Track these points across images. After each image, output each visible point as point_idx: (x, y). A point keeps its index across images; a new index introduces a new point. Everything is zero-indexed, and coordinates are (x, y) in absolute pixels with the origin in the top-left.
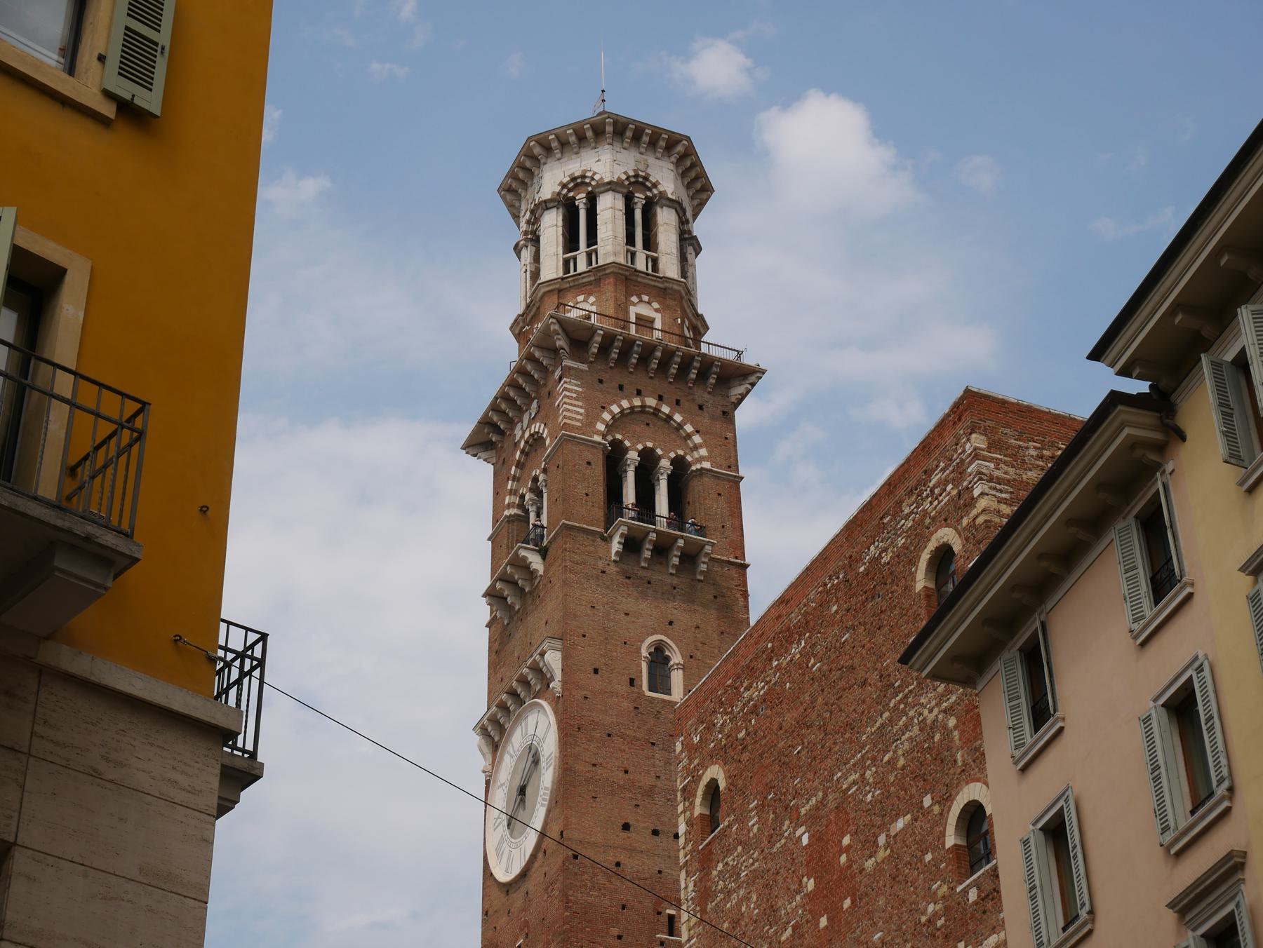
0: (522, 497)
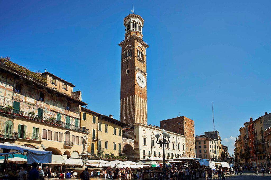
0: (126, 52)
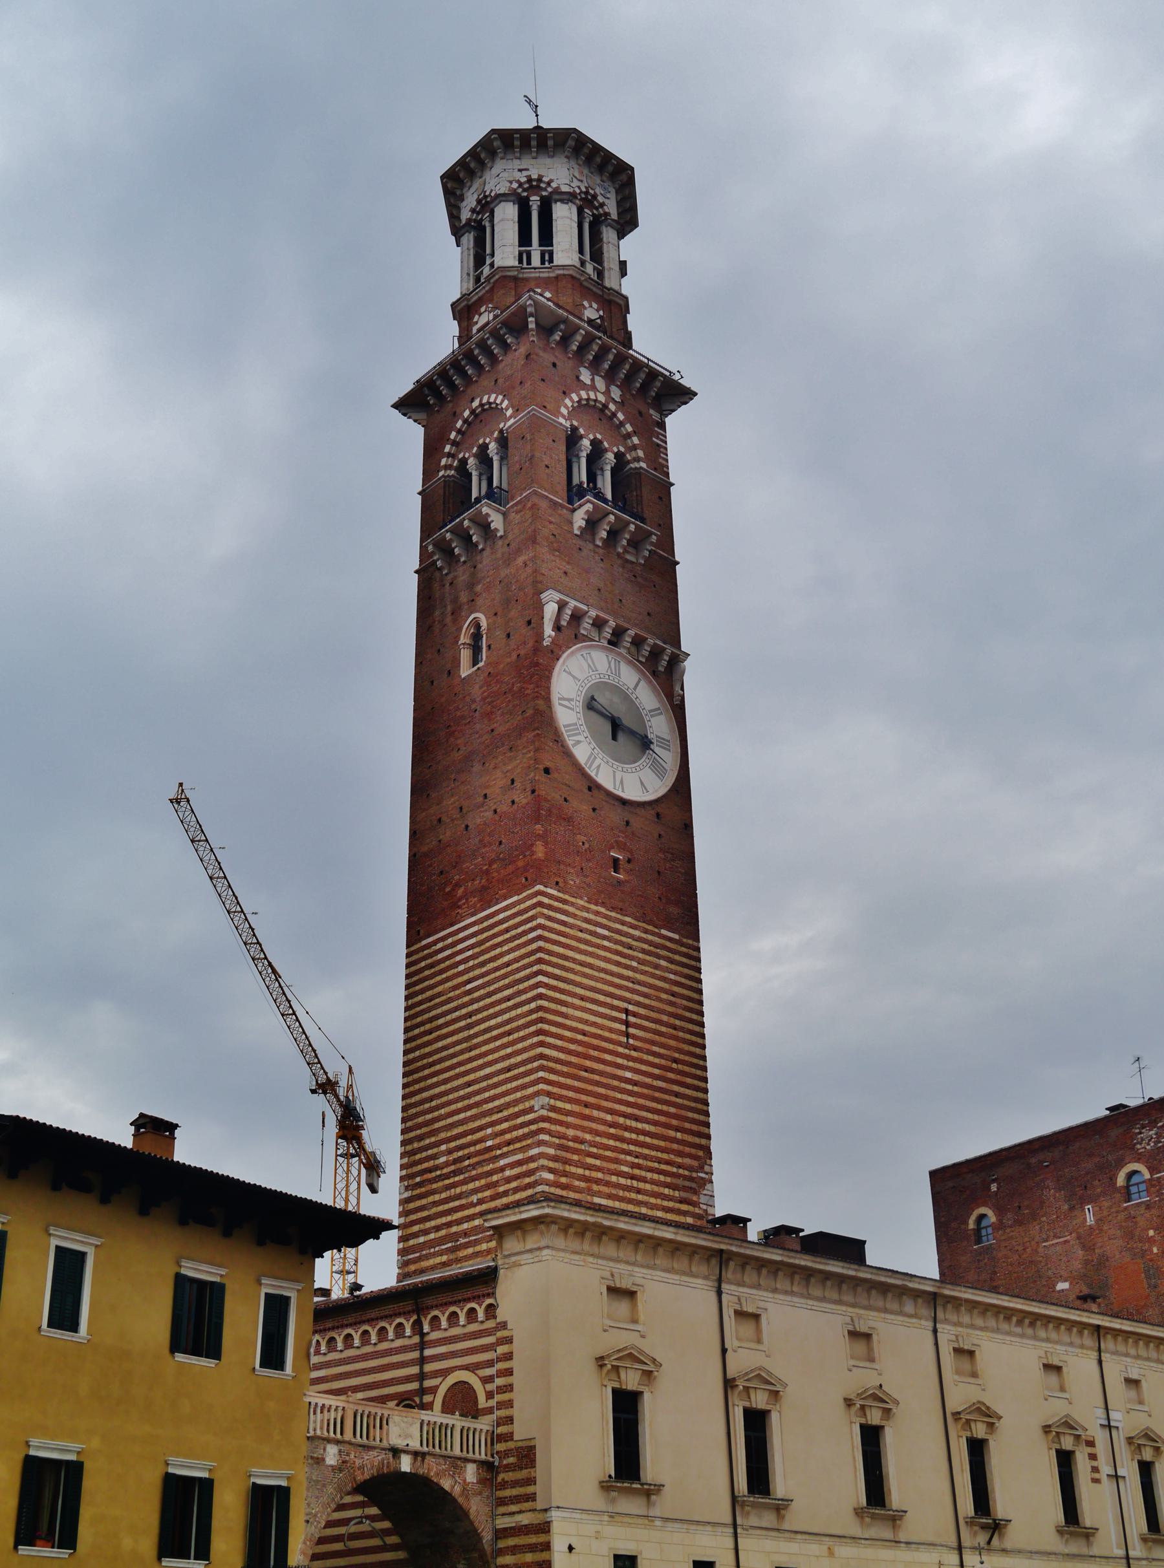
0: (464, 462)
